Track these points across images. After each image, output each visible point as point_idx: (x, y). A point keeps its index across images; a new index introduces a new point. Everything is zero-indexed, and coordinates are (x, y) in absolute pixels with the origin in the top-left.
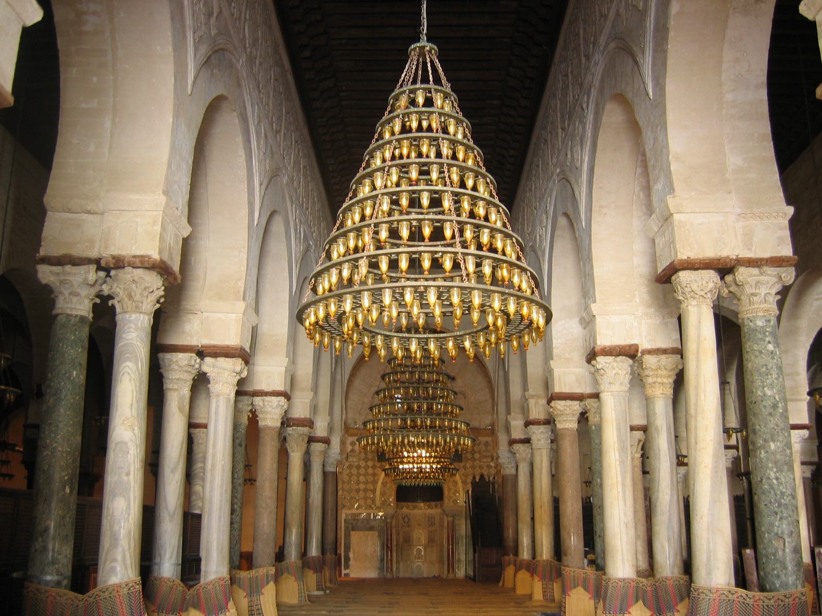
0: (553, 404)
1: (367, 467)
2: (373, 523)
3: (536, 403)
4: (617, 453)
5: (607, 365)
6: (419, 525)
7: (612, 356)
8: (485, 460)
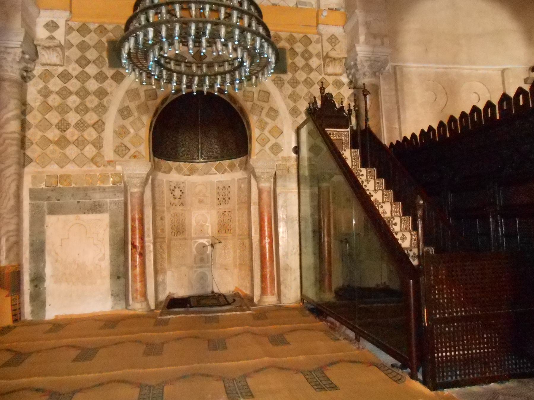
1: (83, 77)
2: (97, 197)
6: (201, 202)
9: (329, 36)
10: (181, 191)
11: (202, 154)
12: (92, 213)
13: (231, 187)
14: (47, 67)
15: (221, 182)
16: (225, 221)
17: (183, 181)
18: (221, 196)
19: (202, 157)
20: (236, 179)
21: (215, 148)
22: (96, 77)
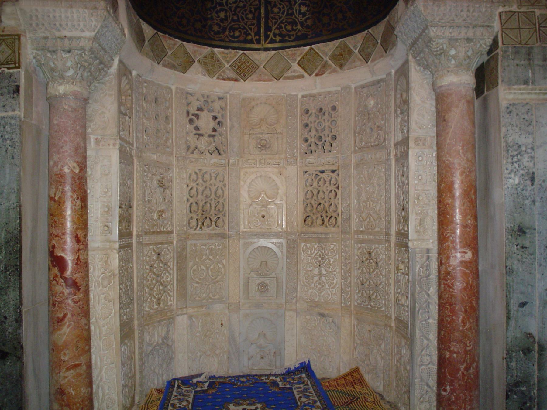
6: (263, 147)
10: (215, 118)
11: (268, 29)
13: (340, 108)
15: (313, 96)
16: (321, 195)
17: (221, 95)
18: (313, 133)
20: (353, 87)
21: (300, 13)
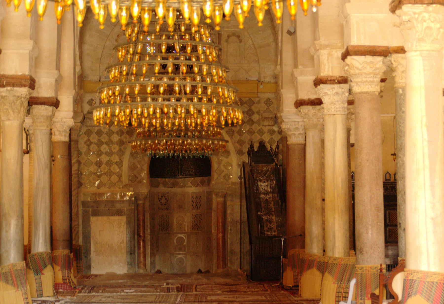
0: (349, 59)
2: (118, 206)
3: (330, 55)
4: (425, 129)
5: (417, 16)
7: (422, 3)
8: (266, 123)
9: (265, 99)
11: (181, 172)
12: (116, 216)
14: (89, 128)
19: (181, 174)
22: (117, 133)
